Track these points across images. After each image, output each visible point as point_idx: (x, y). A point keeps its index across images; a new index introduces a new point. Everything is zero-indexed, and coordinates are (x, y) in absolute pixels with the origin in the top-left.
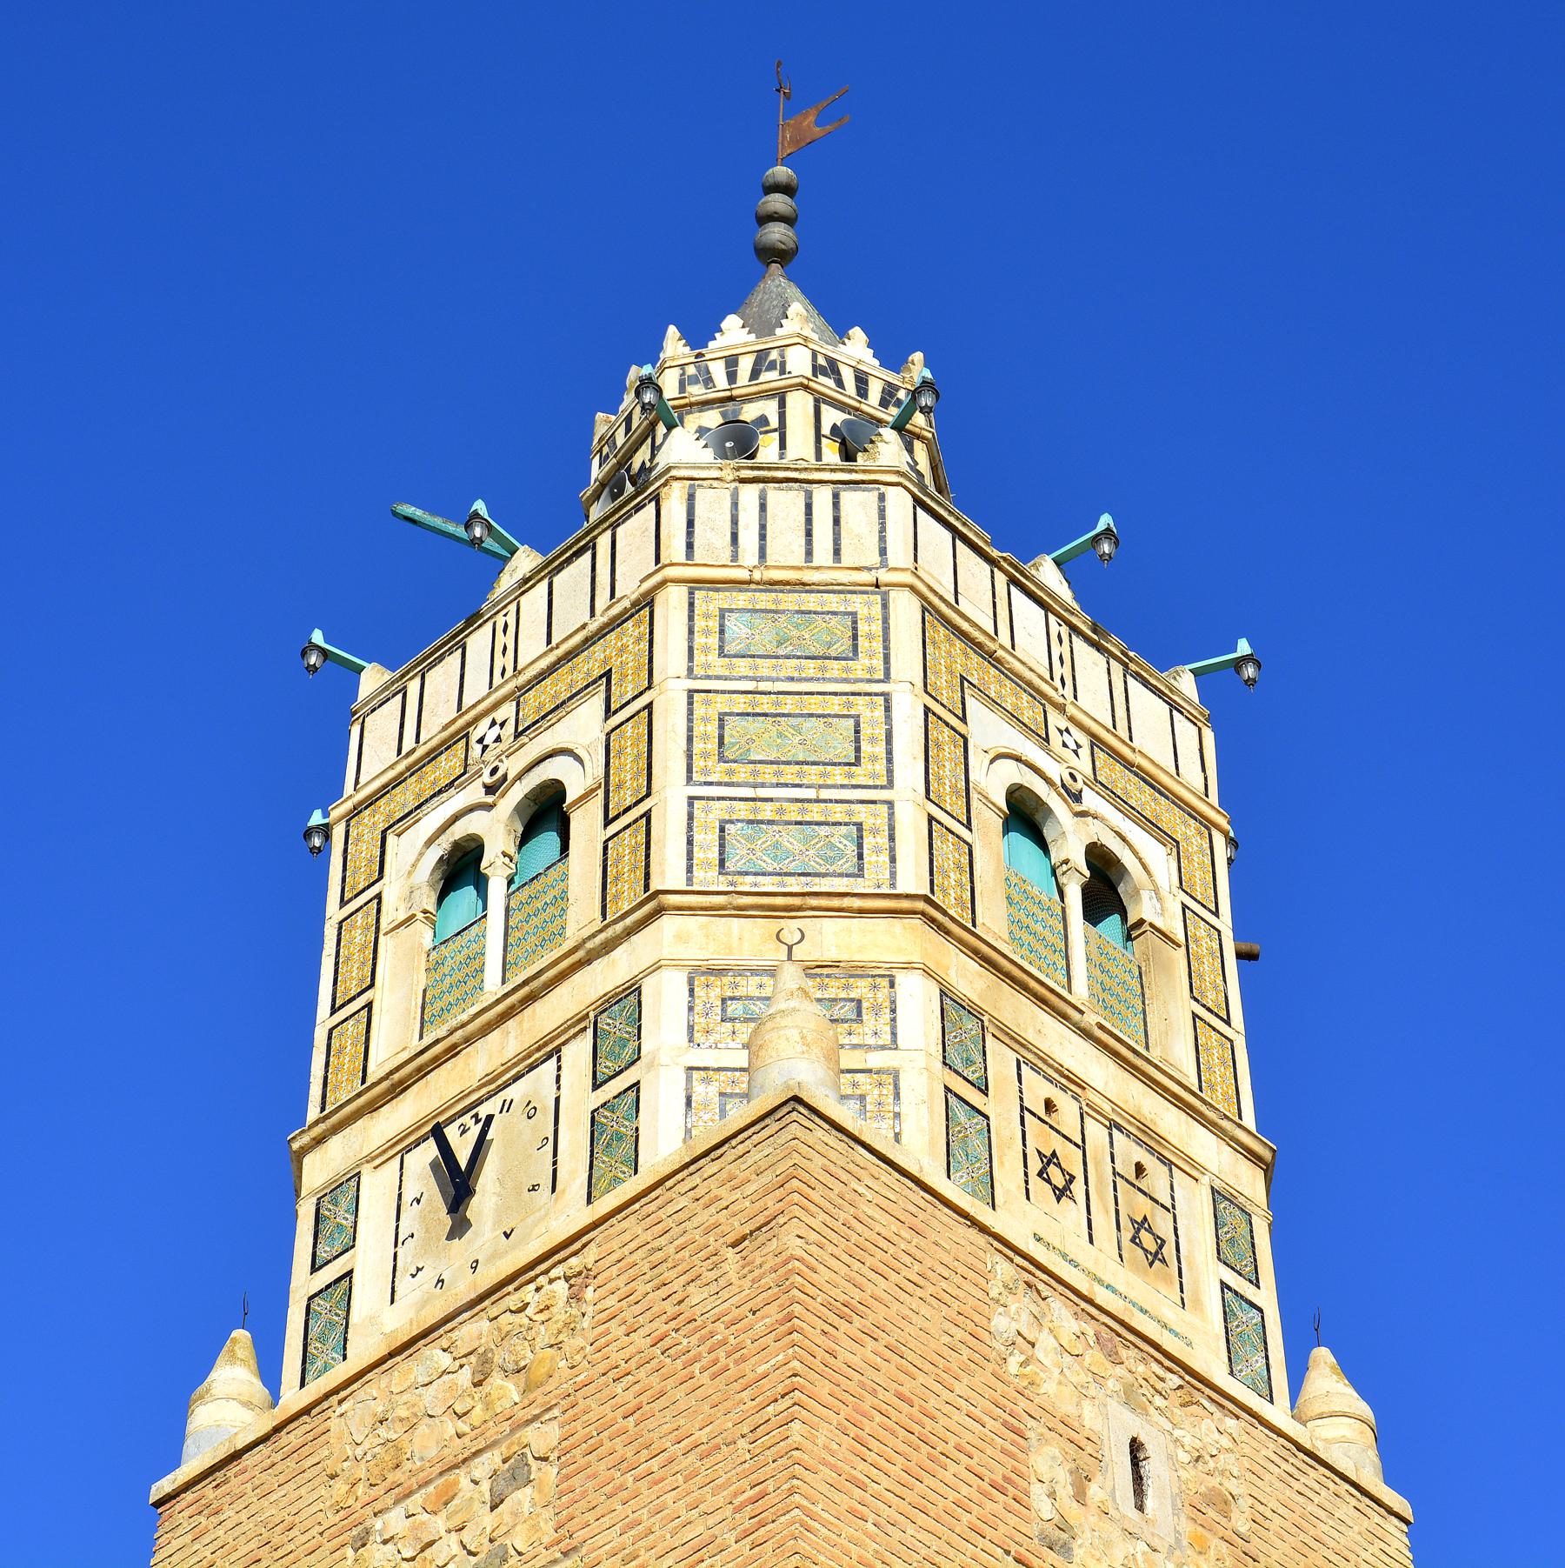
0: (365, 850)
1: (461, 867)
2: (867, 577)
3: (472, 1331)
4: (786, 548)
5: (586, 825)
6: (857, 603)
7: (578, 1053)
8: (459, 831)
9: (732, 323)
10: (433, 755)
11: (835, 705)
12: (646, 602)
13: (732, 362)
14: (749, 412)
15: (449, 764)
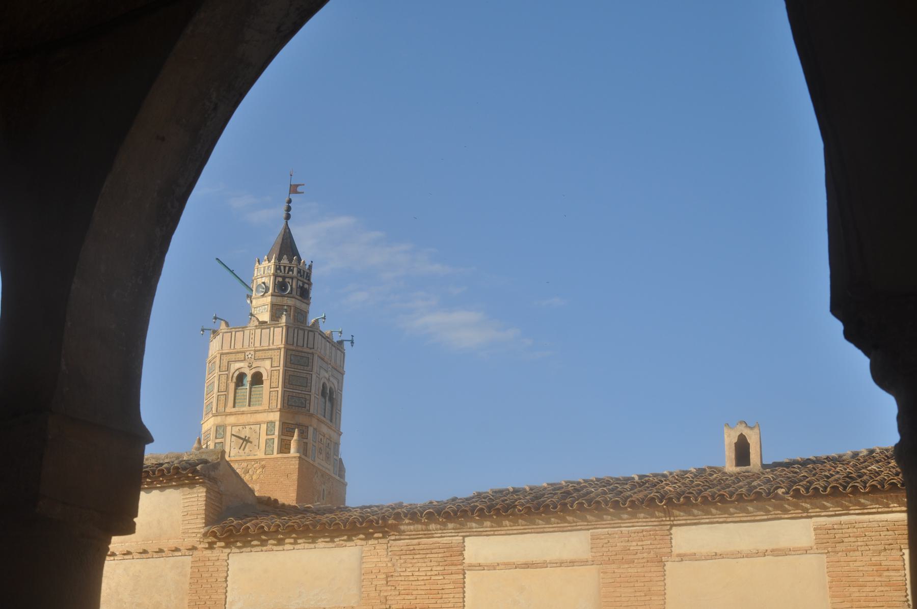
0: (225, 363)
1: (241, 377)
2: (311, 351)
3: (244, 464)
4: (300, 343)
5: (266, 384)
6: (309, 356)
7: (264, 427)
8: (242, 370)
9: (285, 256)
10: (238, 353)
11: (304, 375)
12: (280, 349)
13: (285, 267)
14: (287, 280)
15: (241, 356)
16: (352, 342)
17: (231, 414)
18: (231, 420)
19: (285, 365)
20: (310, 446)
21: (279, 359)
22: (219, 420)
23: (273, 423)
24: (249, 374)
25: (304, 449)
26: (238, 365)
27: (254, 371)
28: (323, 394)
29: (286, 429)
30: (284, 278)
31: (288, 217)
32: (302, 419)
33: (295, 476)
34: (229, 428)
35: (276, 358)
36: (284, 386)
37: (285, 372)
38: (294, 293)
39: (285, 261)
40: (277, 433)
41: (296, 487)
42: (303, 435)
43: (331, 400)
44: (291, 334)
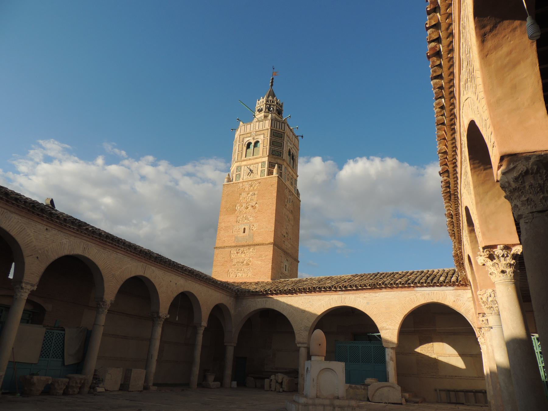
0: (241, 139)
3: (250, 183)
4: (278, 127)
5: (260, 145)
7: (260, 164)
15: (249, 135)
16: (302, 137)
17: (244, 161)
18: (244, 163)
19: (271, 136)
20: (283, 174)
21: (268, 134)
22: (238, 164)
23: (264, 162)
24: (253, 142)
25: (280, 175)
26: (248, 139)
27: (255, 140)
28: (289, 154)
29: (271, 165)
30: (270, 105)
31: (272, 85)
32: (279, 161)
33: (276, 186)
34: (243, 167)
35: (266, 134)
36: (270, 145)
37: (271, 139)
38: (275, 112)
39: (270, 98)
40: (266, 166)
41: (276, 191)
42: (280, 167)
43: (293, 157)
44: (273, 123)
